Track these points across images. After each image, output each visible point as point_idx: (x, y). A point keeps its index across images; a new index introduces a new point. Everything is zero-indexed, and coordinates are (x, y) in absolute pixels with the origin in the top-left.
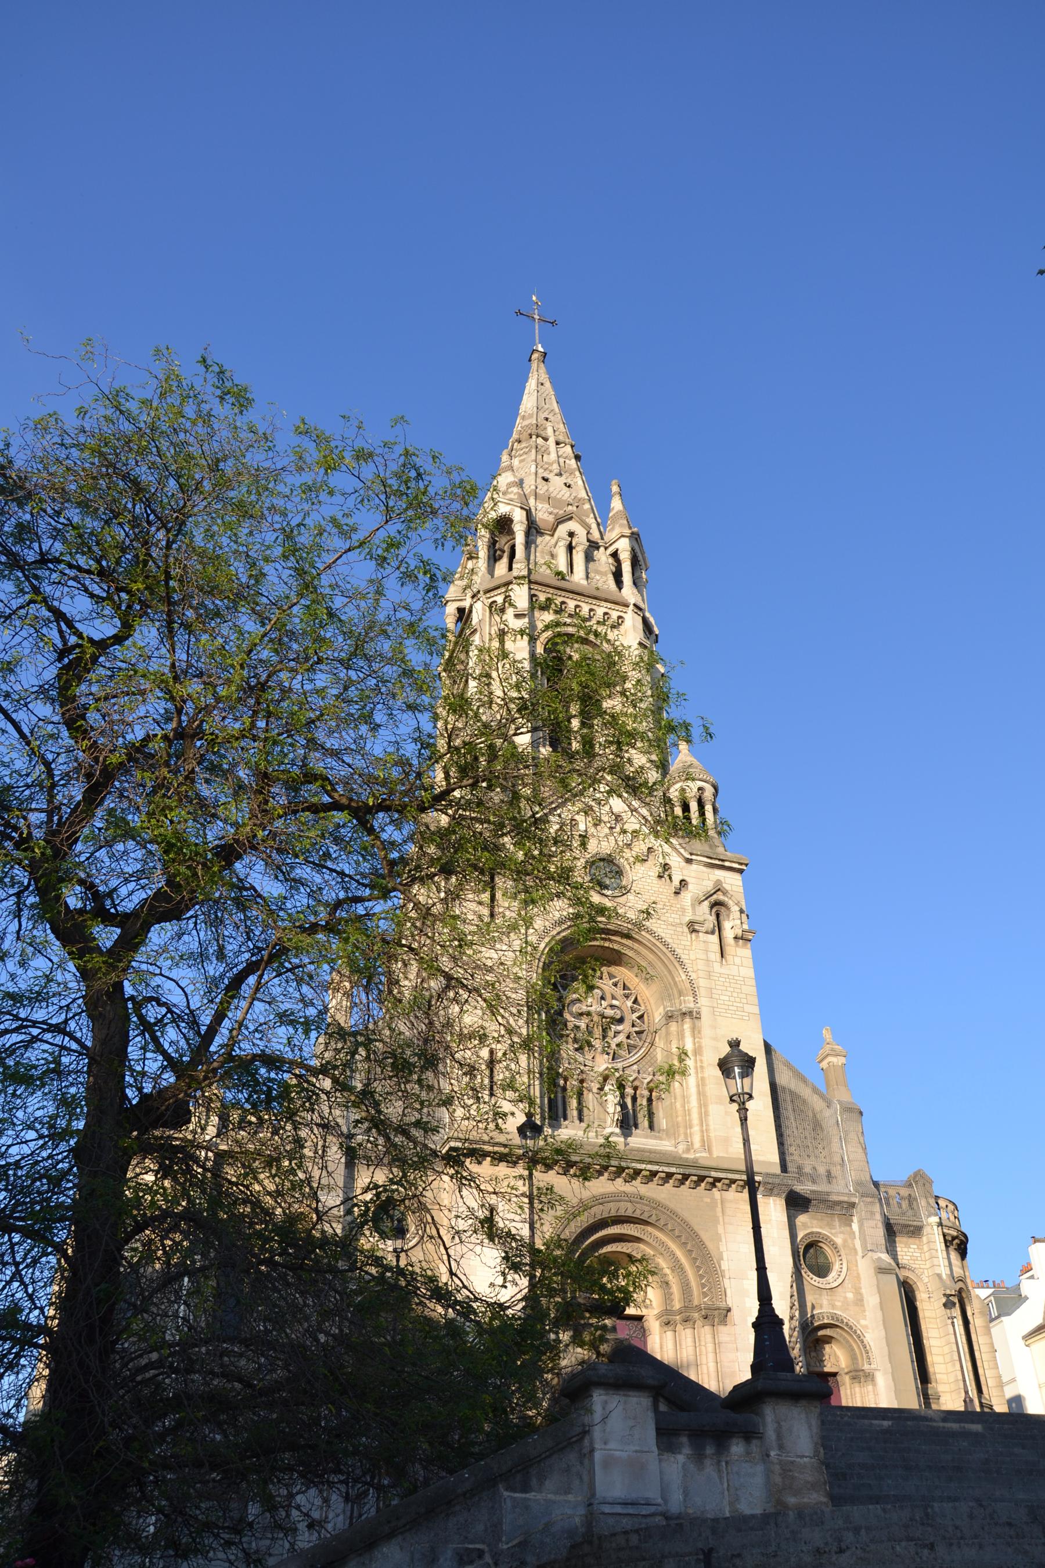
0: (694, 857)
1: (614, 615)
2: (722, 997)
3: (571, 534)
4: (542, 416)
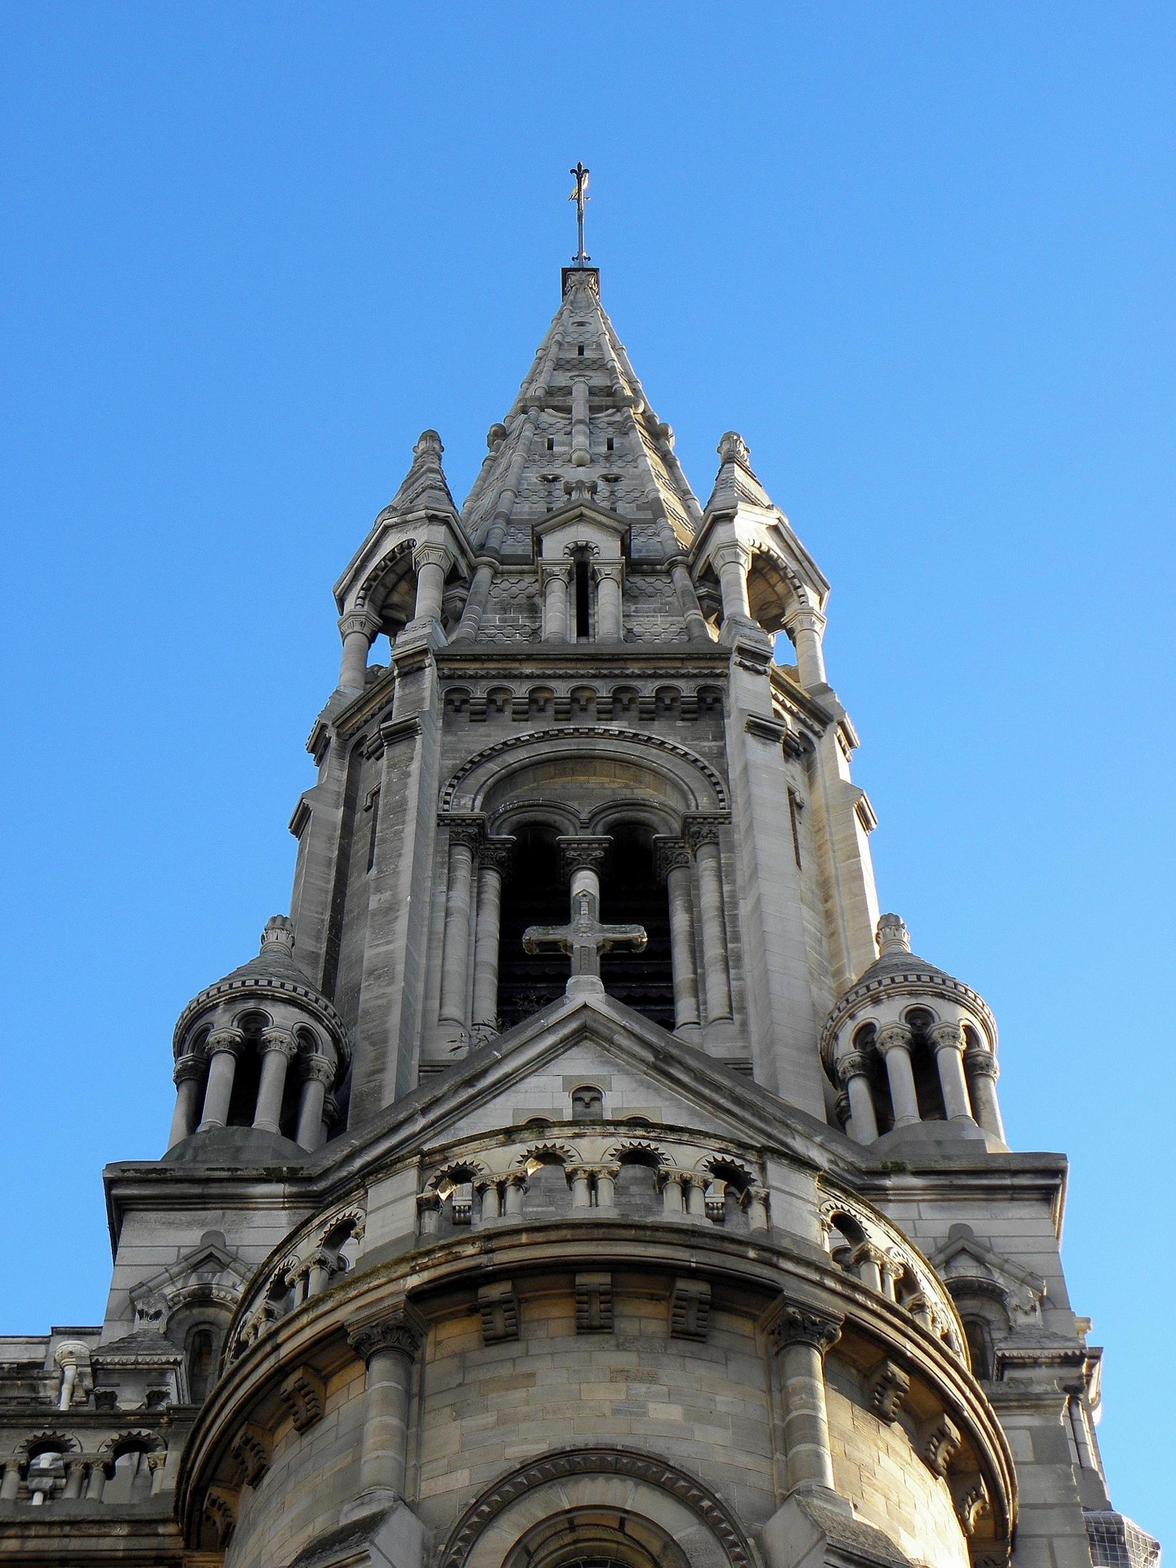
3: (581, 551)
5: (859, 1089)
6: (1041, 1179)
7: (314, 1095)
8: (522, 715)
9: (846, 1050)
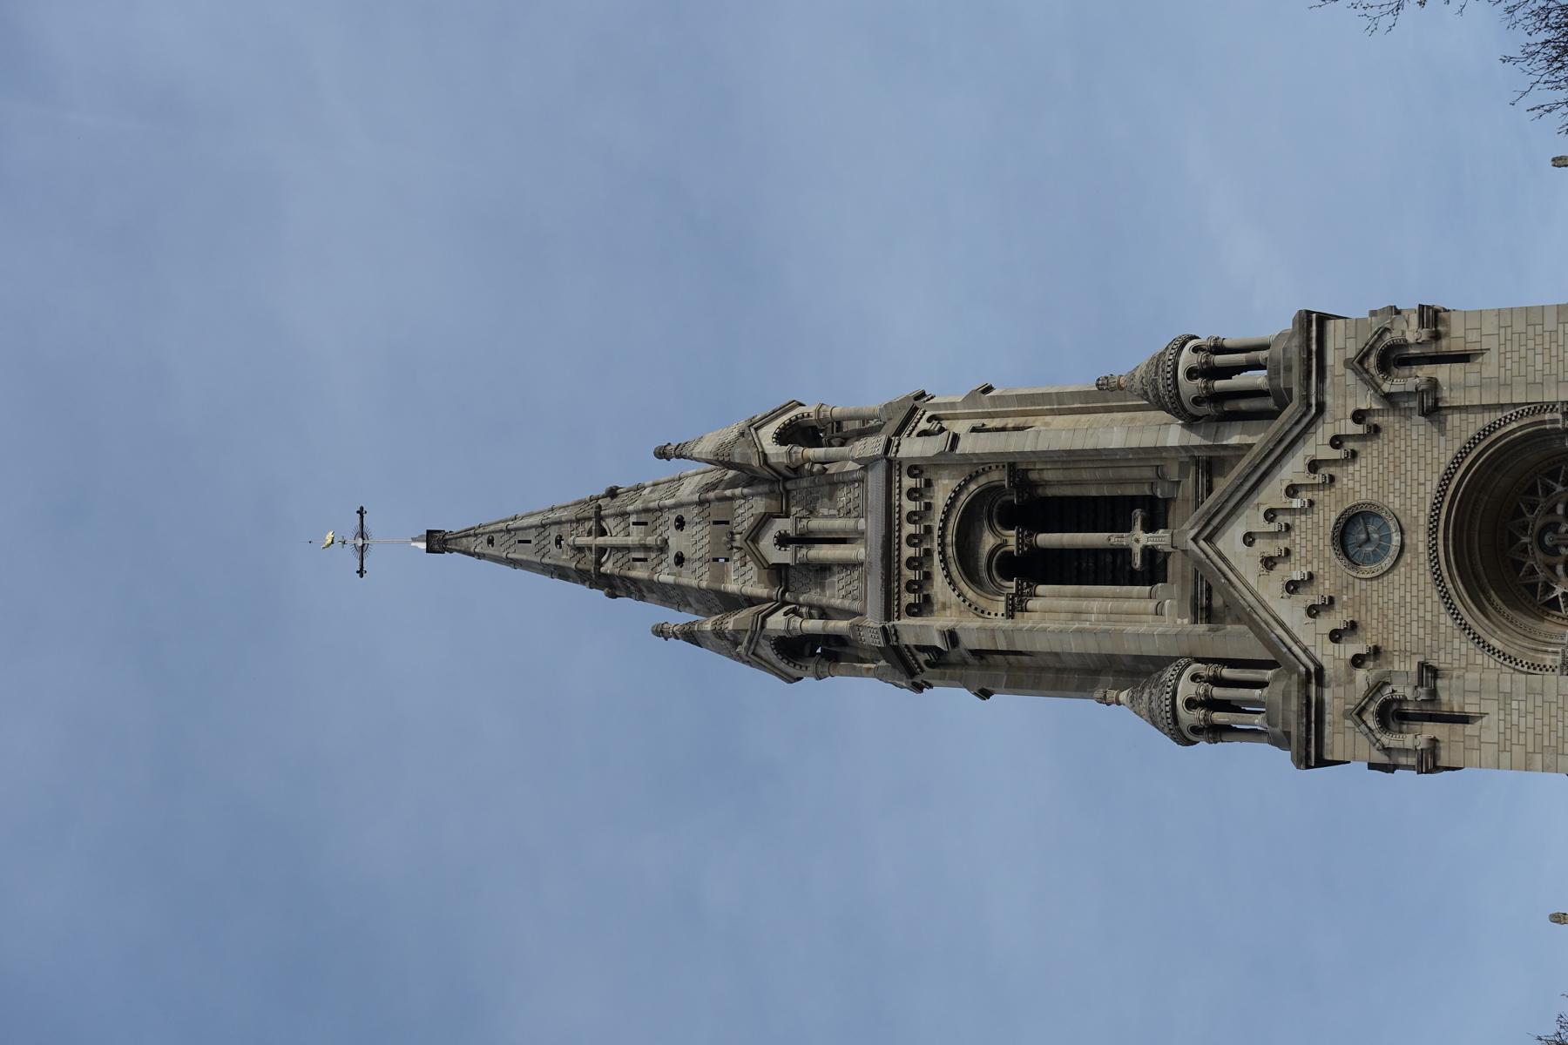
0: (1314, 401)
1: (908, 482)
2: (1539, 367)
3: (783, 540)
4: (554, 550)
5: (1228, 406)
6: (1313, 325)
7: (1227, 673)
8: (928, 576)
9: (1206, 409)
